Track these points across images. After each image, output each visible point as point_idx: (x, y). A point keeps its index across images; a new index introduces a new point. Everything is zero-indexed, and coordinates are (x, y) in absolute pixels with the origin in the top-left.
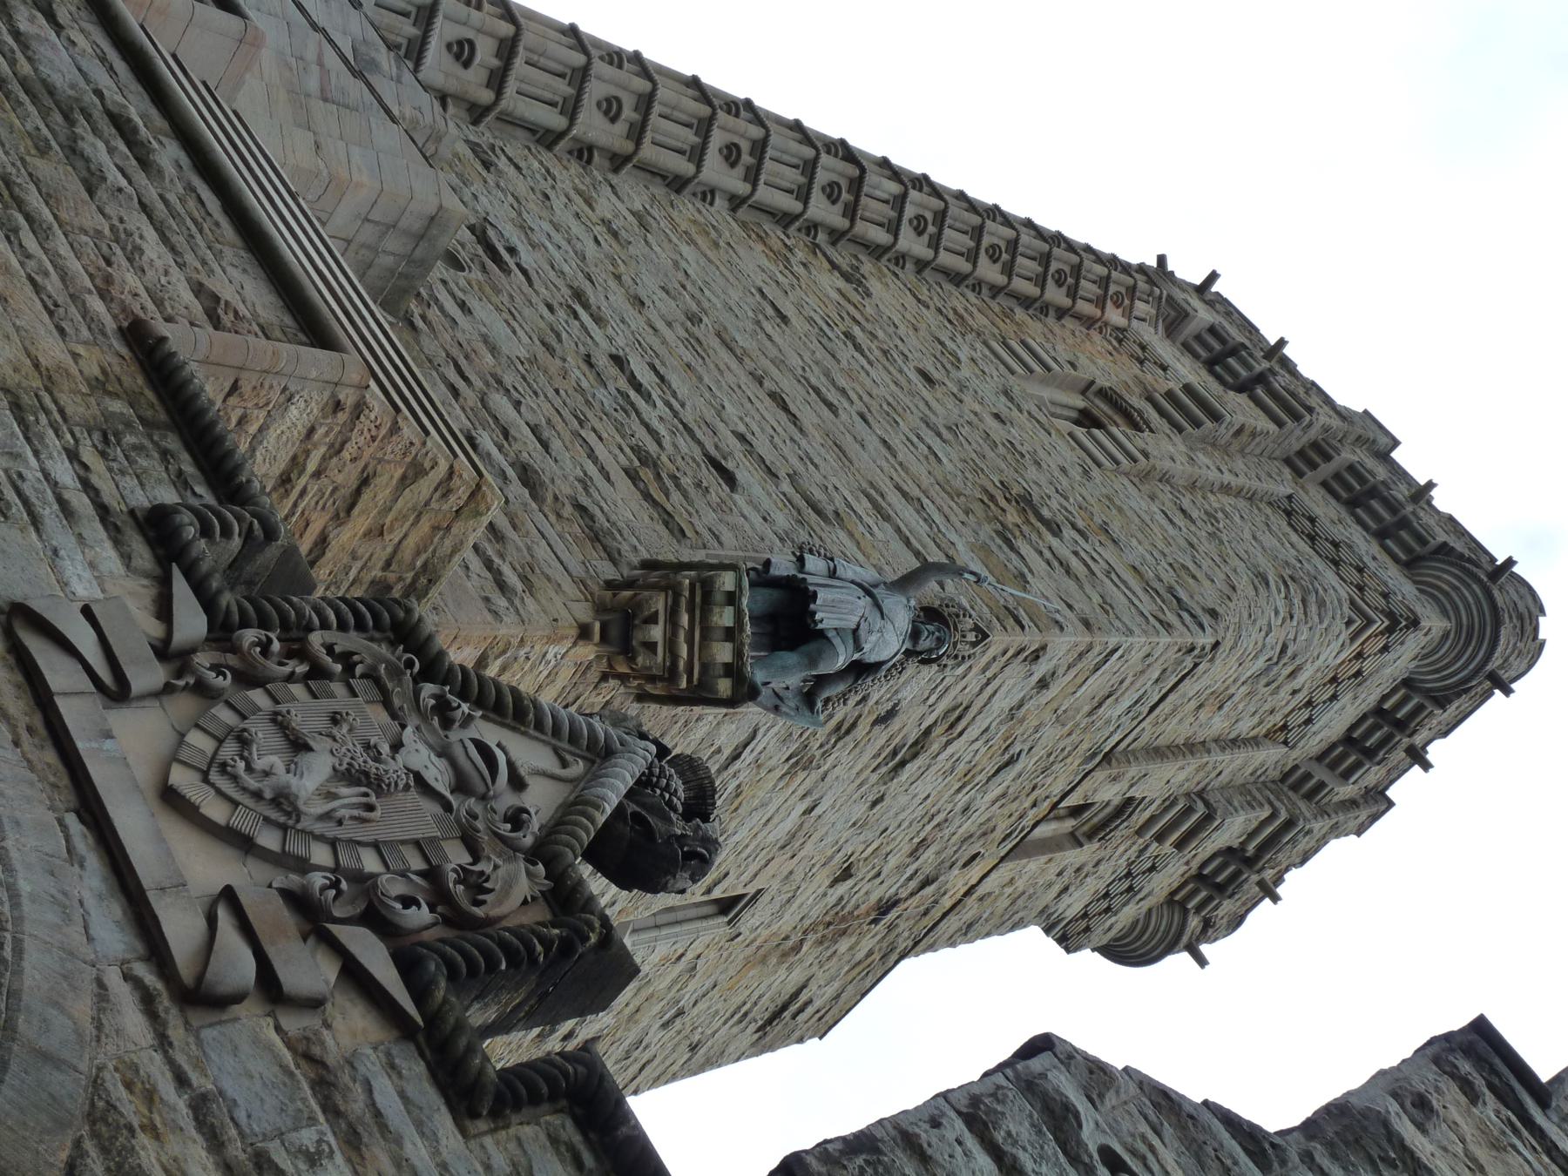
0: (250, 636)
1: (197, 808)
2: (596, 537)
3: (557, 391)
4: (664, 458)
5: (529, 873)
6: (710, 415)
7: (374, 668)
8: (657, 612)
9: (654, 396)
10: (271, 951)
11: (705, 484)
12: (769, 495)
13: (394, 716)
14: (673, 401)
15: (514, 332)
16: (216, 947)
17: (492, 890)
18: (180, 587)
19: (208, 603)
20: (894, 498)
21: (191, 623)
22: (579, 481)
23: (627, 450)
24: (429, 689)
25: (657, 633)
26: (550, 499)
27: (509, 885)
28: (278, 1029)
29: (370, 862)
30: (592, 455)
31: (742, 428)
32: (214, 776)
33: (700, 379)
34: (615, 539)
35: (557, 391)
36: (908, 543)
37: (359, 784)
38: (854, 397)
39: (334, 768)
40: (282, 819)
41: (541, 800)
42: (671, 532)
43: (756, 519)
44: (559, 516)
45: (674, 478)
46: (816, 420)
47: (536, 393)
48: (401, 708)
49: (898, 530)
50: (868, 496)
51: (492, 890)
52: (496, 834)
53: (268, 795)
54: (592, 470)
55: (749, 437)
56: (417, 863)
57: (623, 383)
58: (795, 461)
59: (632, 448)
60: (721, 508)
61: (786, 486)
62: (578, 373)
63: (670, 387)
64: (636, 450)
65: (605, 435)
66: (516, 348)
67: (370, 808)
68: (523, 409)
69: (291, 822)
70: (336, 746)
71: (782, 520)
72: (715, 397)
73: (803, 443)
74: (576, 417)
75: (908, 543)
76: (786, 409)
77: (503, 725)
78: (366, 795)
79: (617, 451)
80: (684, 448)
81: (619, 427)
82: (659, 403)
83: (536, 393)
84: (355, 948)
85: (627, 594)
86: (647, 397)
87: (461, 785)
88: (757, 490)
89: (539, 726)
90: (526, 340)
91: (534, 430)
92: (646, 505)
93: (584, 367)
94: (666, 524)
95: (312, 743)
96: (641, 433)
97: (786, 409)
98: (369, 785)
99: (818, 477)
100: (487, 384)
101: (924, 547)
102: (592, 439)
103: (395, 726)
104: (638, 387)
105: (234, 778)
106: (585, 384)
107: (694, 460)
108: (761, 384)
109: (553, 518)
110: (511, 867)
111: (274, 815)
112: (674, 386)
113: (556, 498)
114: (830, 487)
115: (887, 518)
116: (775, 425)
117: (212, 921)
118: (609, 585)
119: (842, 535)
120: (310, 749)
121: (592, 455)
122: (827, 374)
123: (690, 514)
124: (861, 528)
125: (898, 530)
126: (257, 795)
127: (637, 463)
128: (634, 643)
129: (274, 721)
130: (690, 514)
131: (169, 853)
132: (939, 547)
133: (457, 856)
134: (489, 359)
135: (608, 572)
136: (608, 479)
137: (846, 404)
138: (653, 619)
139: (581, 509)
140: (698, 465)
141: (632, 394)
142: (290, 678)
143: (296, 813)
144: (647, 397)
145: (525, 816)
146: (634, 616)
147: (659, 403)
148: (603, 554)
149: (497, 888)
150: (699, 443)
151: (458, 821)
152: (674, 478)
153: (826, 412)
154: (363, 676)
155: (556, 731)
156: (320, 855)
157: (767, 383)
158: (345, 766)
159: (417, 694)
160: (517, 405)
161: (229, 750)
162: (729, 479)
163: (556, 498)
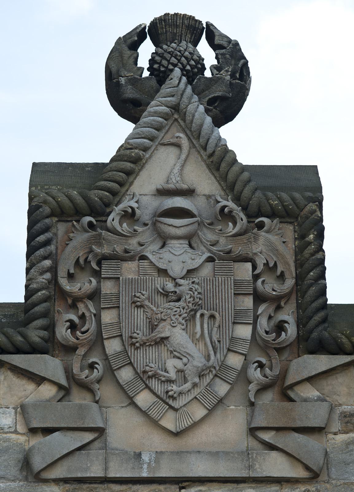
0: (63, 332)
1: (195, 423)
5: (268, 232)
7: (96, 255)
10: (299, 424)
13: (132, 259)
16: (290, 452)
17: (275, 264)
18: (17, 360)
19: (34, 350)
21: (51, 366)
24: (113, 220)
27: (274, 250)
28: (335, 434)
29: (244, 332)
32: (176, 404)
37: (194, 317)
39: (184, 330)
40: (211, 376)
41: (205, 183)
48: (126, 251)
51: (275, 264)
52: (235, 236)
53: (197, 380)
56: (248, 302)
67: (212, 317)
69: (214, 372)
70: (168, 321)
77: (137, 175)
78: (202, 315)
84: (306, 374)
87: (190, 239)
89: (145, 149)
95: (163, 335)
98: (196, 311)
103: (145, 263)
105: (180, 393)
110: (261, 241)
111: (208, 379)
117: (272, 447)
120: (167, 338)
126: (195, 385)
129: (137, 348)
131: (227, 453)
133: (245, 271)
142: (98, 317)
143: (210, 368)
145: (226, 210)
149: (275, 259)
151: (221, 259)
154: (99, 264)
155: (152, 139)
156: (235, 361)
158: (183, 322)
159: (114, 232)
161: (154, 384)
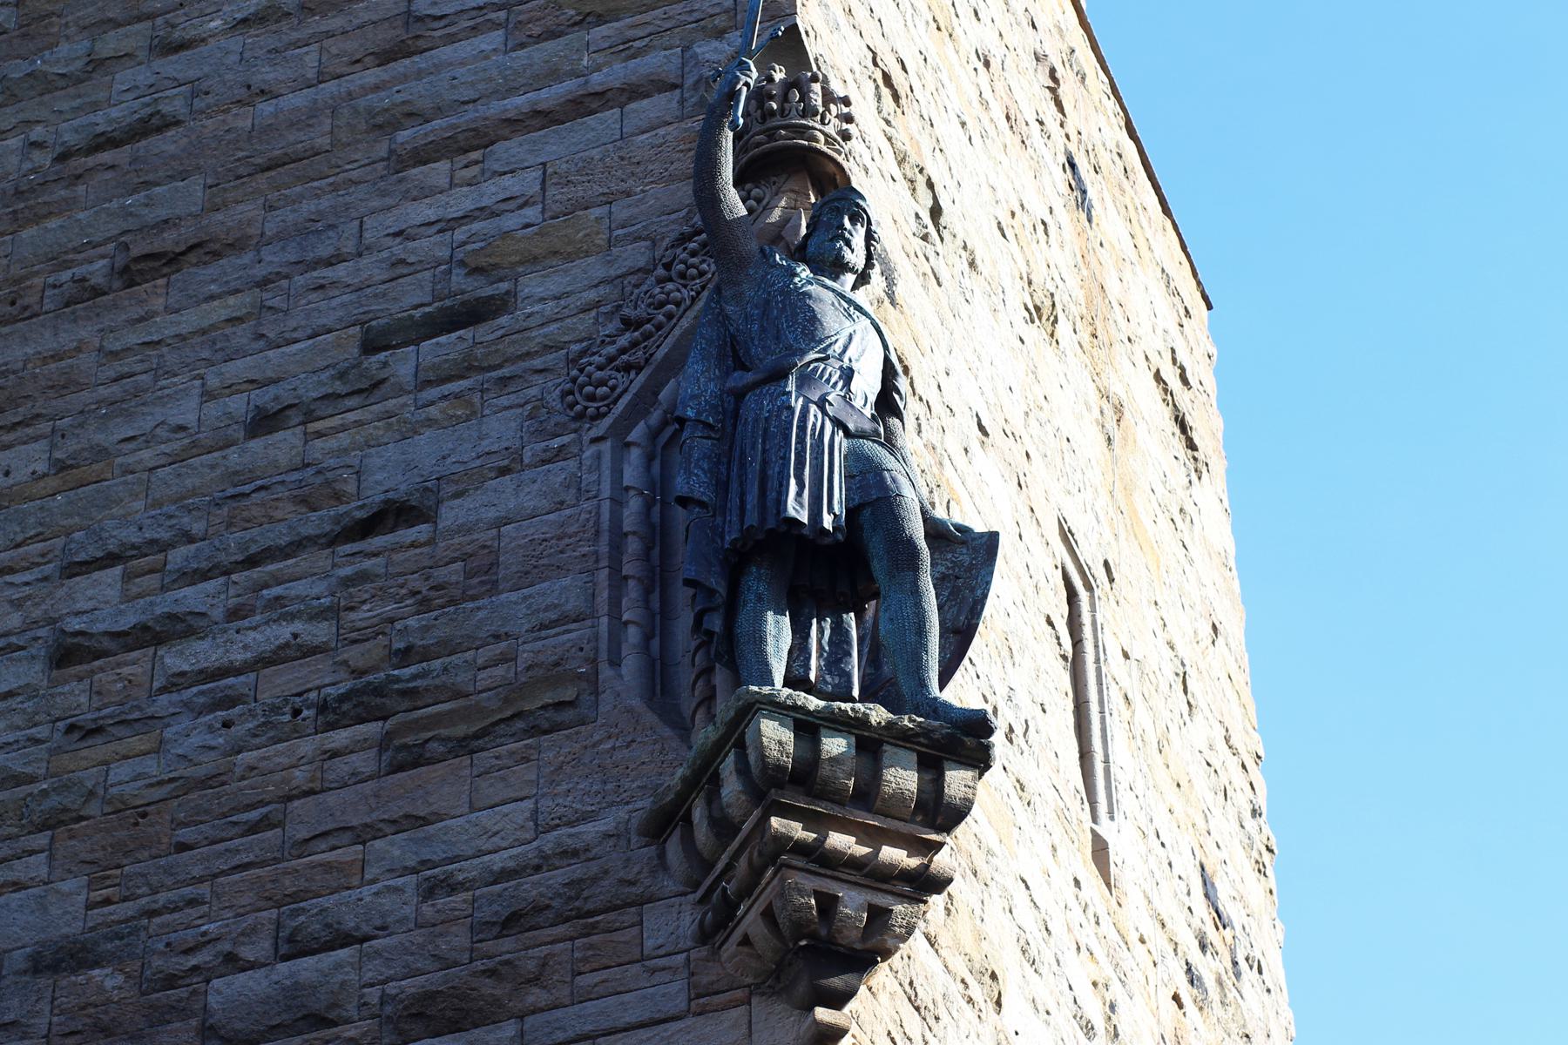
2: (579, 913)
3: (183, 847)
4: (354, 654)
6: (202, 473)
8: (818, 894)
9: (165, 604)
11: (415, 582)
12: (430, 422)
14: (178, 556)
15: (18, 886)
20: (410, 83)
22: (429, 891)
23: (340, 737)
25: (853, 903)
26: (488, 987)
30: (363, 835)
31: (238, 405)
33: (101, 453)
34: (595, 880)
35: (183, 847)
36: (545, 118)
38: (110, 44)
42: (555, 728)
43: (505, 496)
44: (535, 980)
45: (405, 656)
46: (195, 189)
47: (193, 902)
49: (515, 124)
50: (421, 156)
54: (394, 848)
55: (265, 398)
57: (136, 664)
58: (331, 309)
59: (331, 726)
60: (484, 572)
61: (402, 364)
62: (120, 772)
63: (140, 550)
64: (331, 714)
65: (299, 776)
66: (67, 909)
68: (247, 953)
71: (501, 428)
72: (148, 439)
73: (273, 259)
74: (254, 828)
75: (545, 118)
76: (173, 260)
79: (341, 767)
80: (312, 589)
81: (271, 732)
82: (192, 597)
83: (193, 902)
85: (750, 920)
86: (179, 628)
88: (427, 450)
90: (37, 866)
91: (295, 947)
92: (484, 759)
93: (99, 749)
94: (535, 731)
96: (280, 683)
97: (173, 260)
99: (370, 268)
100: (180, 1011)
101: (554, 75)
102: (304, 817)
104: (148, 636)
106: (151, 766)
107: (347, 582)
108: (97, 292)
109: (536, 996)
112: (132, 536)
113: (491, 973)
114: (398, 249)
115: (481, 139)
116: (217, 312)
118: (710, 934)
119: (533, 285)
121: (363, 835)
122: (45, 84)
123: (503, 659)
124: (510, 222)
125: (515, 124)
127: (372, 729)
128: (858, 946)
130: (503, 659)
132: (552, 35)
134: (107, 979)
135: (669, 923)
136: (425, 821)
137: (125, 77)
138: (828, 904)
139: (512, 922)
140: (363, 577)
141: (176, 659)
144: (179, 628)
146: (812, 936)
147: (192, 597)
148: (630, 915)
150: (297, 546)
152: (405, 656)
153: (166, 144)
157: (97, 271)
160: (233, 963)
162: (394, 514)
163: (491, 973)
